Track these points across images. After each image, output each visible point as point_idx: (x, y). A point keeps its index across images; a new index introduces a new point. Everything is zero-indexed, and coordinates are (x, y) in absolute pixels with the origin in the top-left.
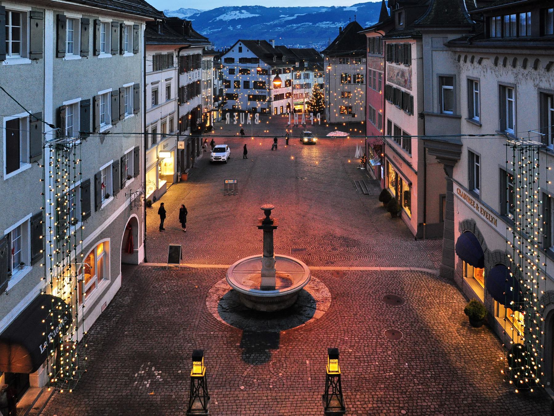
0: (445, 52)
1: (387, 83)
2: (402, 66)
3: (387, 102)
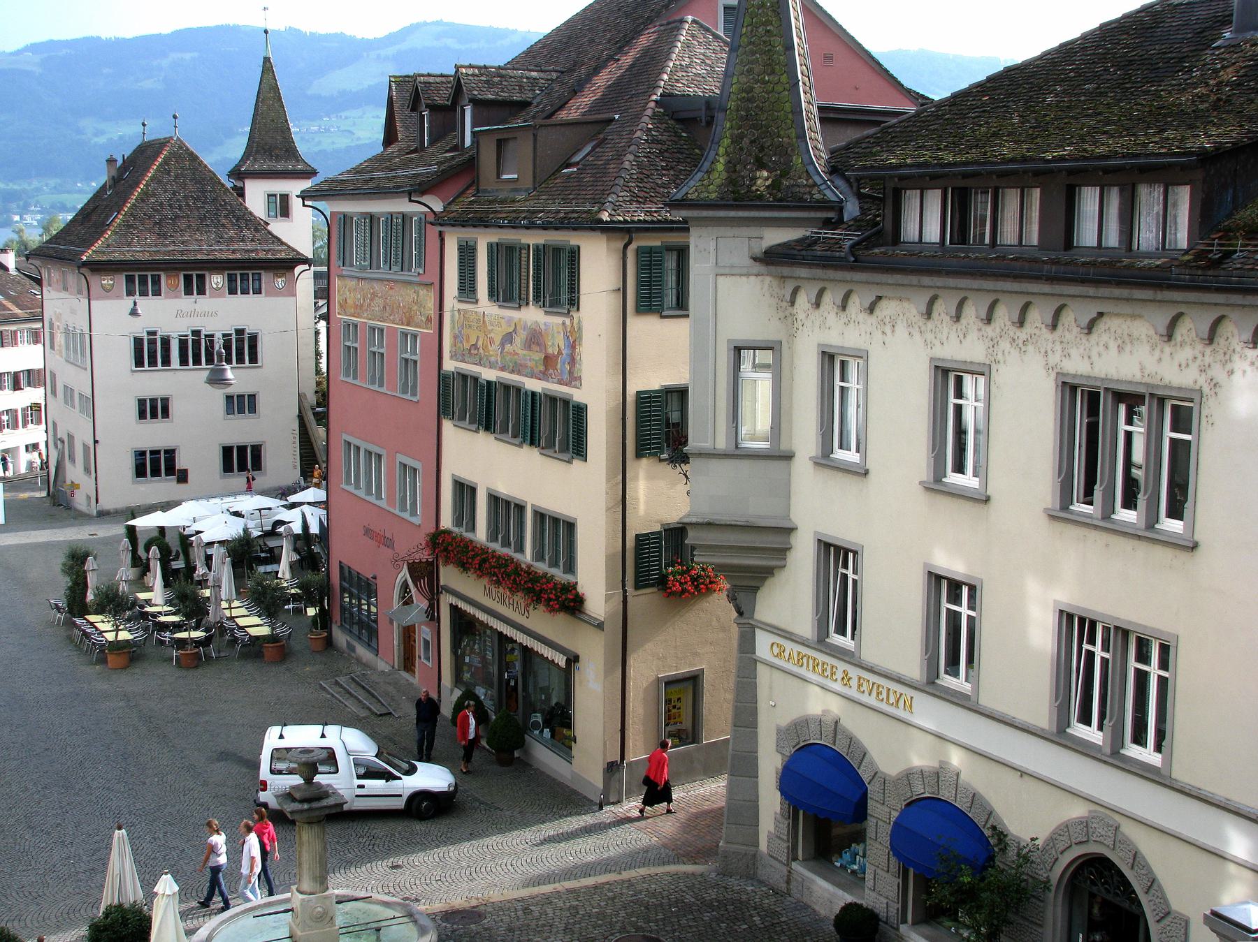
0: (753, 278)
1: (449, 365)
2: (533, 315)
3: (447, 425)
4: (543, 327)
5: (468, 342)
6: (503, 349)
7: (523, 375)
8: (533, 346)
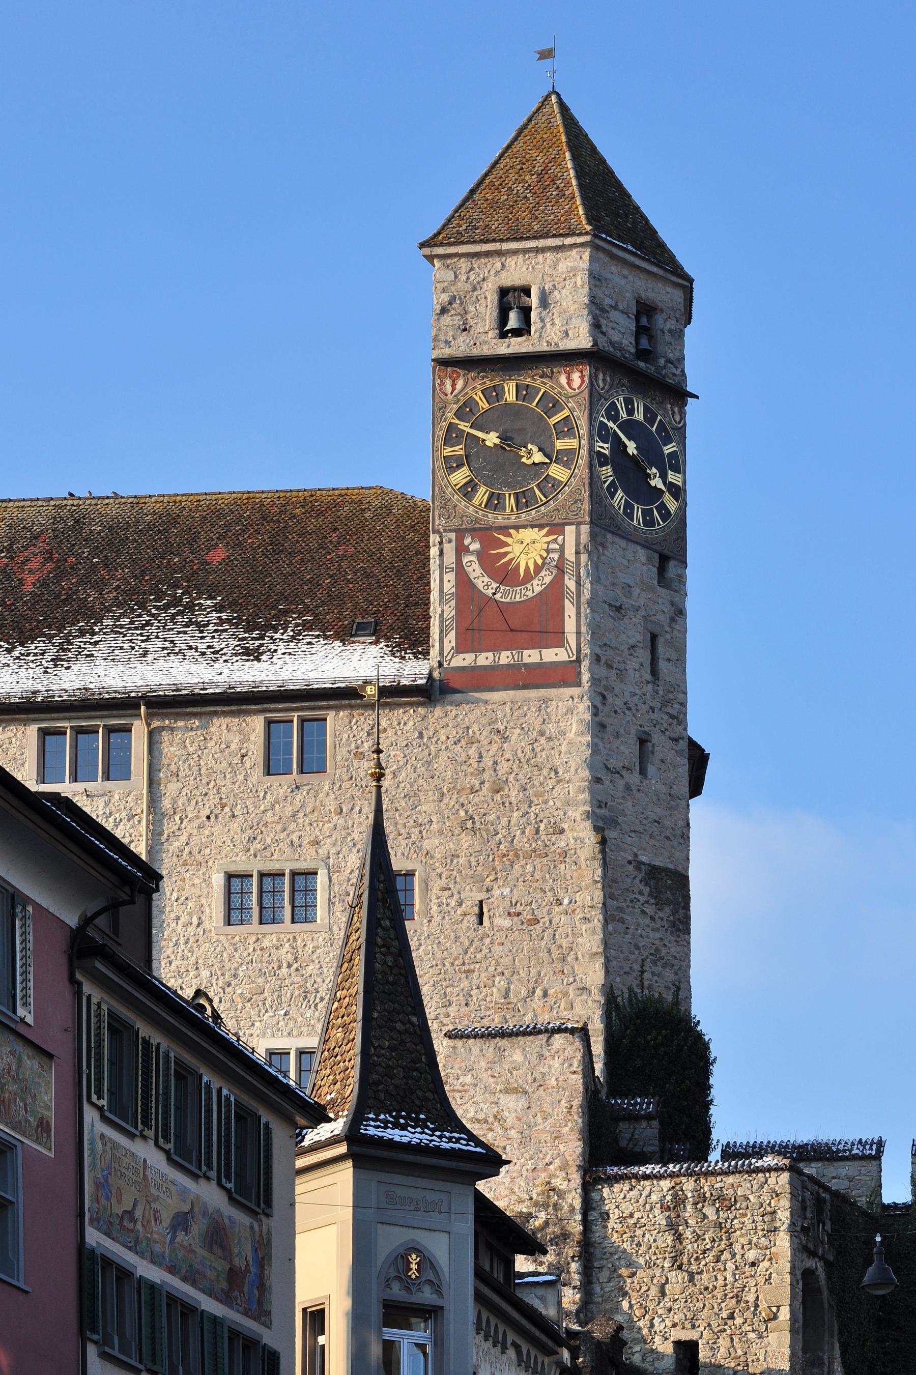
3: (92, 1350)
4: (227, 1221)
5: (119, 1202)
6: (174, 1237)
7: (200, 1289)
8: (215, 1247)
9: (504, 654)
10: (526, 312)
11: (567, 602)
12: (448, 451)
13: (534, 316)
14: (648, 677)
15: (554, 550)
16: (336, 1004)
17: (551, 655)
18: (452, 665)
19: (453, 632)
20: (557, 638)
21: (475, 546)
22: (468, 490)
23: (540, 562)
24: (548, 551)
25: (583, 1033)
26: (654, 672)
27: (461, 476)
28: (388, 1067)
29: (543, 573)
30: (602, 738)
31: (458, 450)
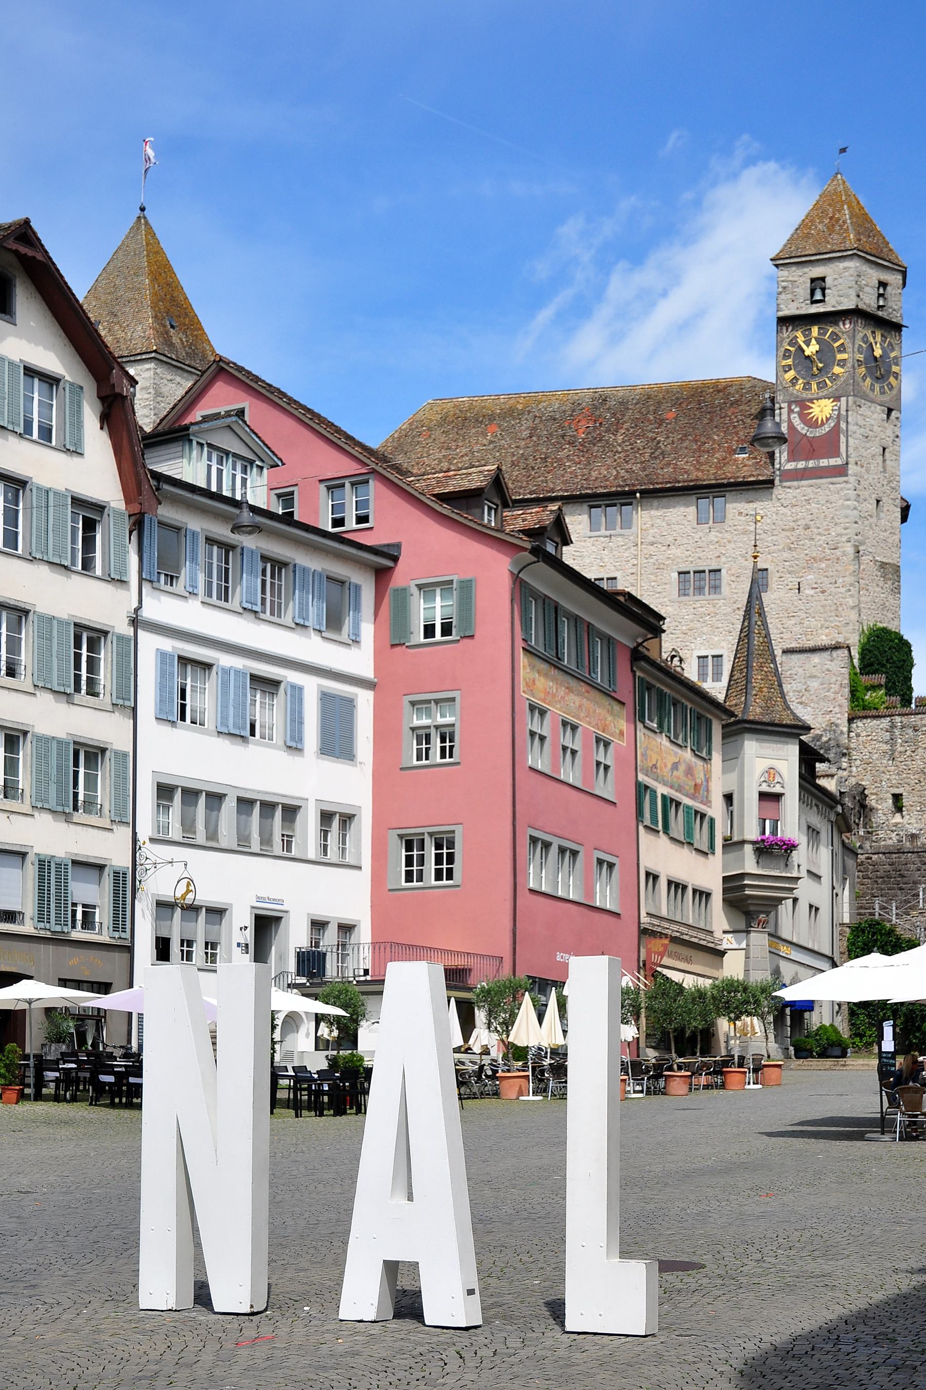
5: (651, 760)
9: (811, 462)
10: (823, 290)
11: (841, 435)
12: (784, 363)
13: (827, 291)
14: (882, 470)
15: (836, 410)
16: (737, 660)
17: (833, 462)
18: (786, 468)
19: (786, 453)
20: (837, 454)
21: (797, 409)
22: (794, 381)
23: (828, 416)
24: (832, 410)
25: (848, 648)
26: (884, 467)
27: (791, 374)
28: (760, 688)
29: (830, 421)
30: (858, 501)
31: (789, 361)
